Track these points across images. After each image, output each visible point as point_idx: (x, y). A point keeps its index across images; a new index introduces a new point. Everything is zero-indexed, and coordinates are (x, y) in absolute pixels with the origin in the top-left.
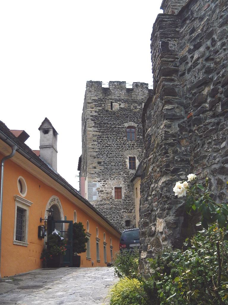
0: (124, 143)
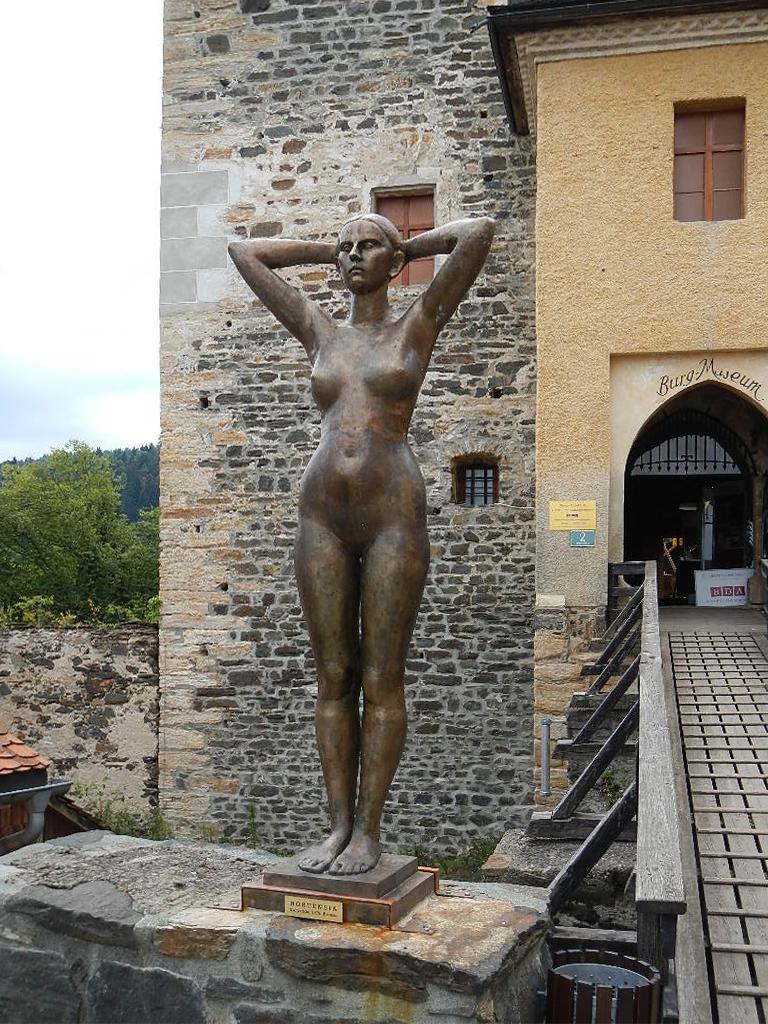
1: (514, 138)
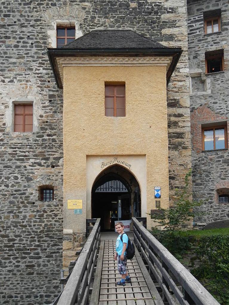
1: (58, 89)
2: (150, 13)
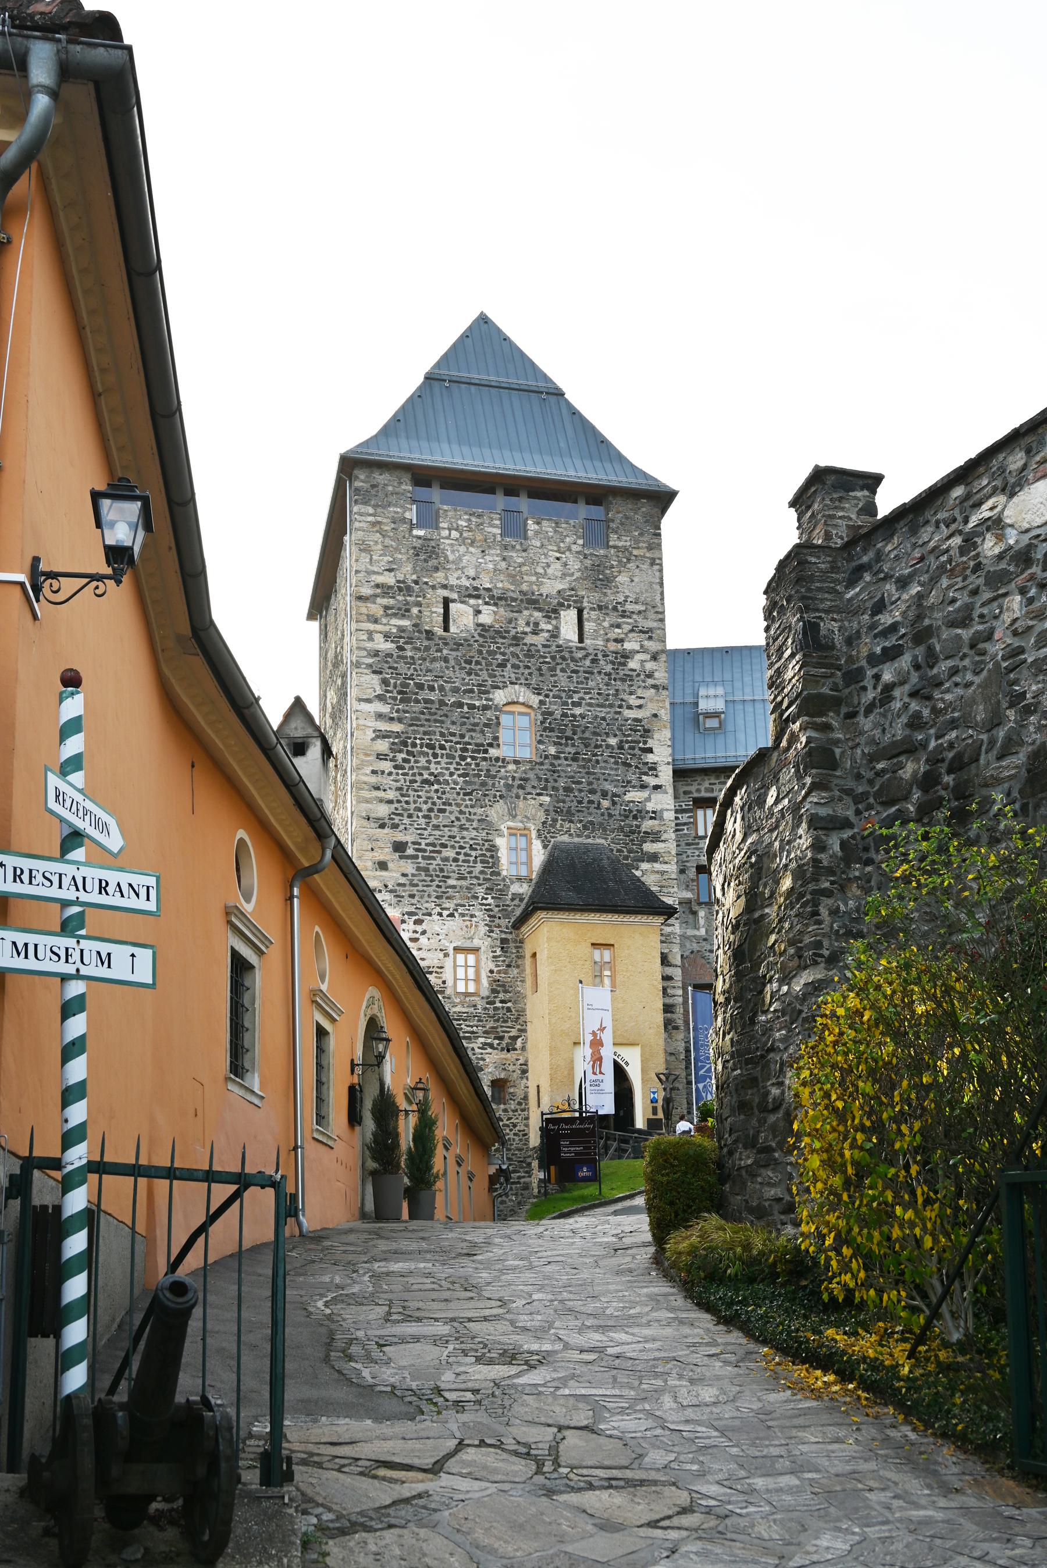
0: (488, 771)
2: (627, 817)
